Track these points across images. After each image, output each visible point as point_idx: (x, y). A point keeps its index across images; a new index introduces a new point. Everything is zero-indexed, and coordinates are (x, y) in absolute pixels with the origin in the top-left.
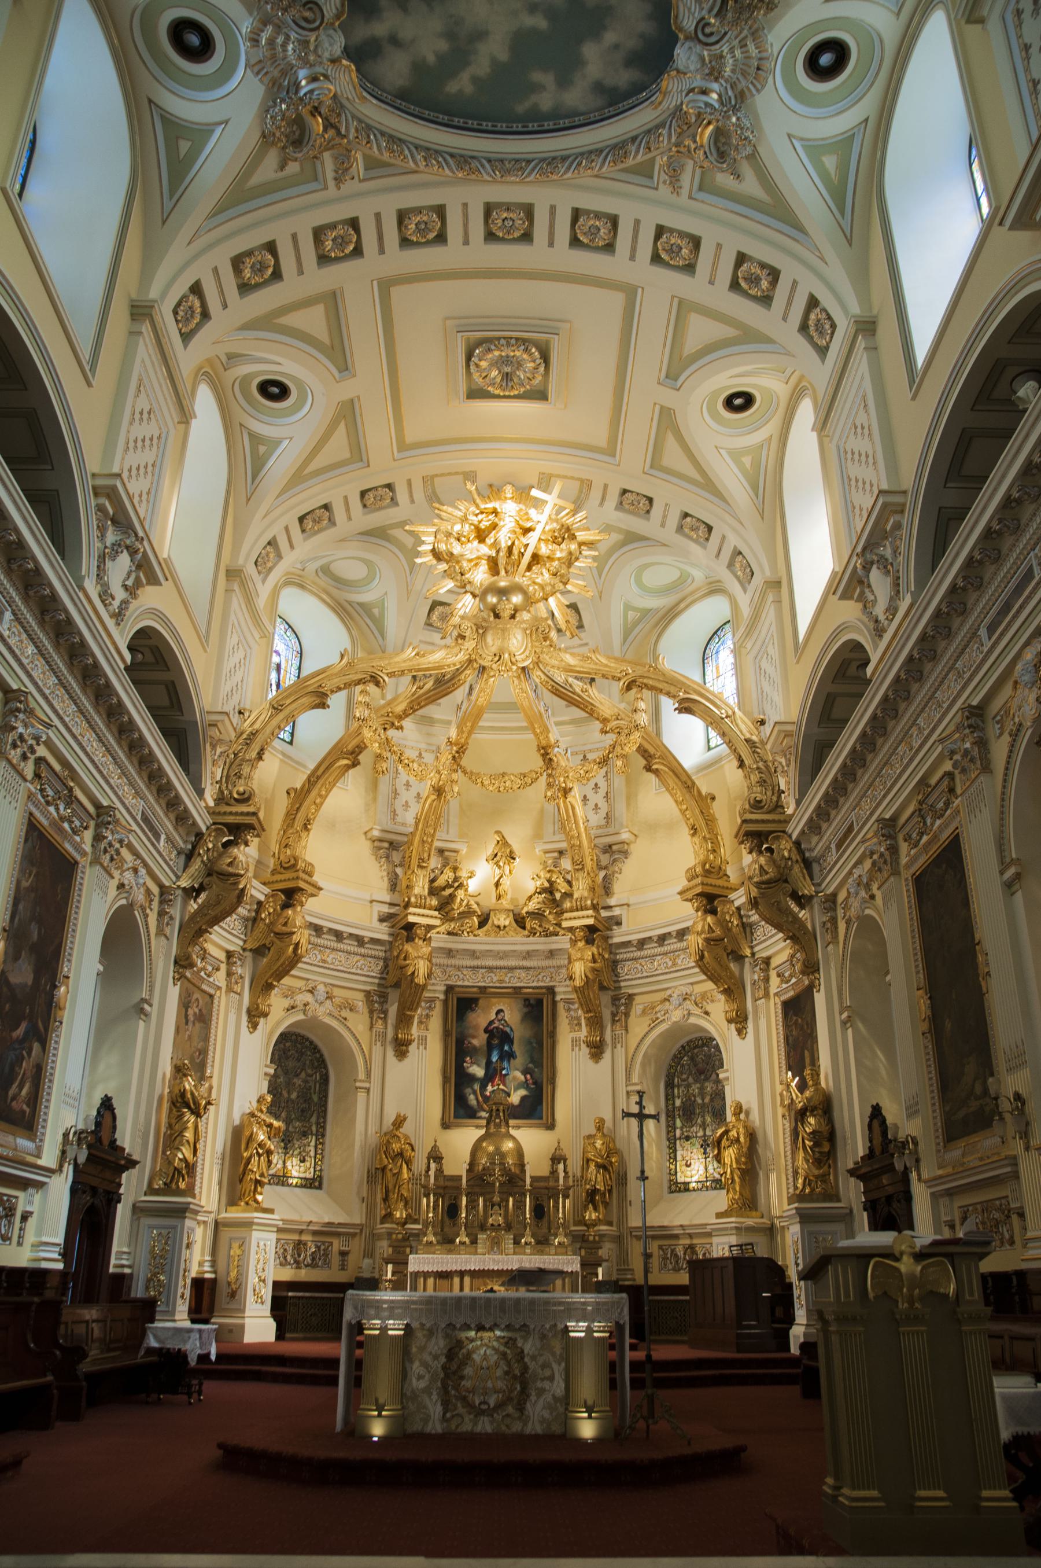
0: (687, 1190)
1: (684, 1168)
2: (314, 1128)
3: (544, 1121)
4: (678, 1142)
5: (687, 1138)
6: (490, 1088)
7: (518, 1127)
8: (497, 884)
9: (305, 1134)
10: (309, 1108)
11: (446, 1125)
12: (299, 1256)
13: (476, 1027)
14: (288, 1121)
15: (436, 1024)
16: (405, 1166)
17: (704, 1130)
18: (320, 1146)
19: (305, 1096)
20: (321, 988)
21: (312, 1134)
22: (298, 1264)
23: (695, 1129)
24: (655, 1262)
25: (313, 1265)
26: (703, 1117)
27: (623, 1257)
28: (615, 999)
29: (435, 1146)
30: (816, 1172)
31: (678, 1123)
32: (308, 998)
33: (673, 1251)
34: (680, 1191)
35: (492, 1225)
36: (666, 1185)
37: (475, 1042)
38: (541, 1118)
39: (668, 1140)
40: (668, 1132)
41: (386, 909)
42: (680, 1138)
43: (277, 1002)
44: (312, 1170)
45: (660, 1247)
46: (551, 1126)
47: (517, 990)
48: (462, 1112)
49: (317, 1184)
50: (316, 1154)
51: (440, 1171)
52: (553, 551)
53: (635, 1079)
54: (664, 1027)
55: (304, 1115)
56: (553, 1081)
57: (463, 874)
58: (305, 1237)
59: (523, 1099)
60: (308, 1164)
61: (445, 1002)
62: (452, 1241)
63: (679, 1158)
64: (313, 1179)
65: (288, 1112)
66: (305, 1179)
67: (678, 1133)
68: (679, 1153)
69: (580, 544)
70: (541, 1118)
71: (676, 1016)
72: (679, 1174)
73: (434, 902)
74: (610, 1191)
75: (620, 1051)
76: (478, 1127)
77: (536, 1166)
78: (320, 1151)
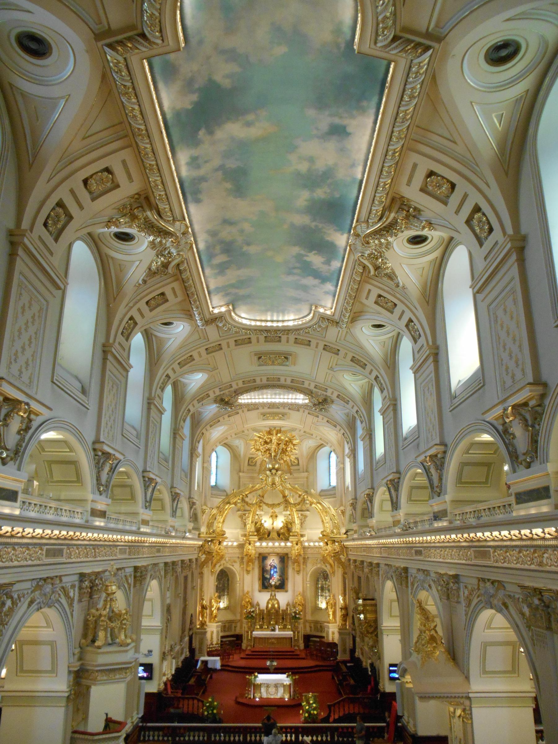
6: (271, 581)
7: (278, 592)
8: (273, 524)
11: (260, 591)
13: (267, 564)
14: (220, 593)
15: (256, 563)
19: (224, 585)
20: (227, 559)
22: (225, 631)
25: (228, 631)
28: (304, 558)
30: (344, 623)
32: (225, 562)
37: (267, 568)
41: (243, 533)
43: (217, 566)
46: (287, 591)
47: (278, 554)
51: (259, 609)
52: (286, 448)
53: (308, 580)
54: (315, 567)
55: (223, 590)
56: (287, 579)
57: (263, 522)
59: (280, 584)
61: (259, 557)
62: (262, 628)
69: (294, 445)
71: (319, 566)
73: (256, 533)
75: (305, 573)
76: (268, 592)
77: (283, 606)
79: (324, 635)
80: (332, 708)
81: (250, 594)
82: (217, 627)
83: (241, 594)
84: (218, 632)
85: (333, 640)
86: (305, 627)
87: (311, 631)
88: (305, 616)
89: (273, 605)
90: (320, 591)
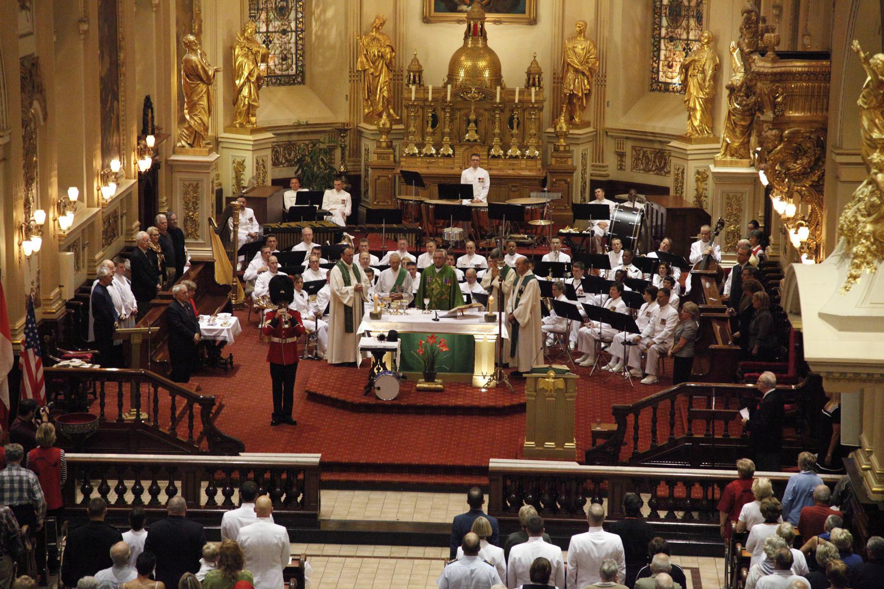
0: (667, 90)
1: (665, 68)
2: (293, 25)
3: (527, 15)
4: (662, 41)
5: (671, 39)
9: (284, 32)
10: (287, 5)
11: (426, 20)
12: (290, 155)
14: (268, 22)
16: (385, 69)
17: (688, 33)
18: (300, 42)
21: (292, 31)
23: (679, 31)
24: (628, 161)
26: (688, 20)
27: (599, 155)
29: (415, 60)
31: (665, 22)
33: (645, 153)
34: (660, 90)
35: (469, 140)
36: (648, 82)
38: (524, 12)
39: (653, 37)
40: (654, 29)
42: (664, 38)
44: (294, 66)
45: (634, 148)
46: (533, 22)
48: (442, 5)
49: (299, 79)
50: (297, 50)
58: (294, 138)
60: (290, 61)
63: (662, 57)
64: (296, 75)
65: (267, 13)
66: (289, 76)
67: (663, 32)
68: (663, 53)
70: (524, 12)
72: (661, 74)
74: (588, 96)
76: (459, 21)
78: (300, 47)
79: (668, 181)
80: (631, 418)
81: (389, 26)
82: (257, 146)
83: (353, 29)
84: (260, 165)
85: (699, 197)
86: (599, 155)
87: (621, 168)
88: (601, 115)
89: (475, 73)
90: (665, 22)
